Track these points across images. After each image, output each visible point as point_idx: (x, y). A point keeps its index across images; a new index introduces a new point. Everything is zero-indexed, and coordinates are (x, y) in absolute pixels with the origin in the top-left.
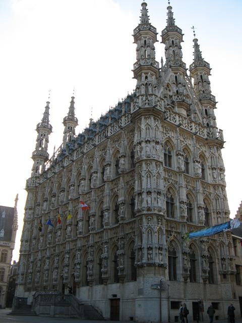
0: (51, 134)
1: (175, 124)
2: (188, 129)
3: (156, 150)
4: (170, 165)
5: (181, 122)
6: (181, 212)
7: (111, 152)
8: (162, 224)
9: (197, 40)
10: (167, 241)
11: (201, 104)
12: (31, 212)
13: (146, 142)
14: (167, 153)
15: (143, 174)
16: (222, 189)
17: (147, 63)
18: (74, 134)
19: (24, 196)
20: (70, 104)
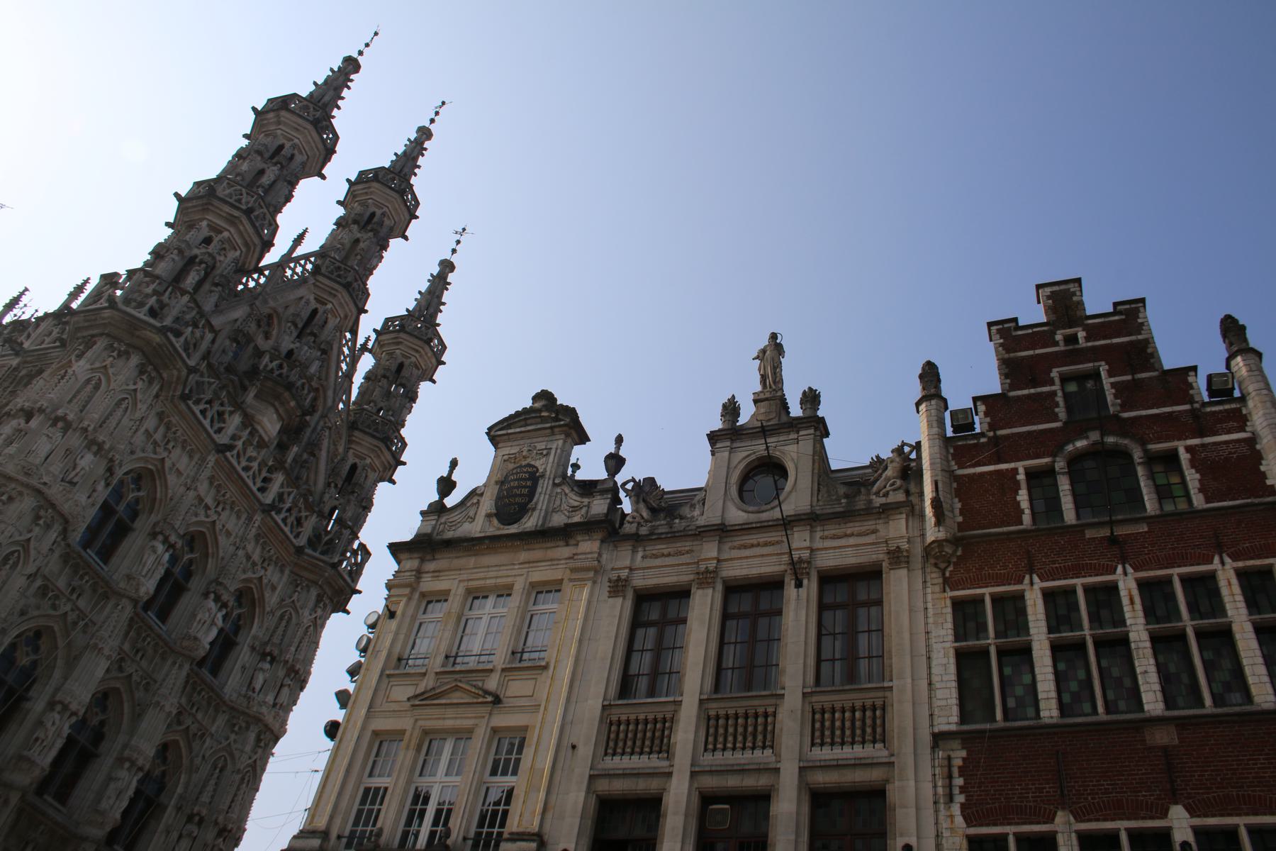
1: (215, 436)
2: (250, 483)
3: (74, 468)
4: (106, 554)
11: (350, 442)
13: (56, 421)
14: (121, 508)
16: (258, 740)
17: (239, 201)
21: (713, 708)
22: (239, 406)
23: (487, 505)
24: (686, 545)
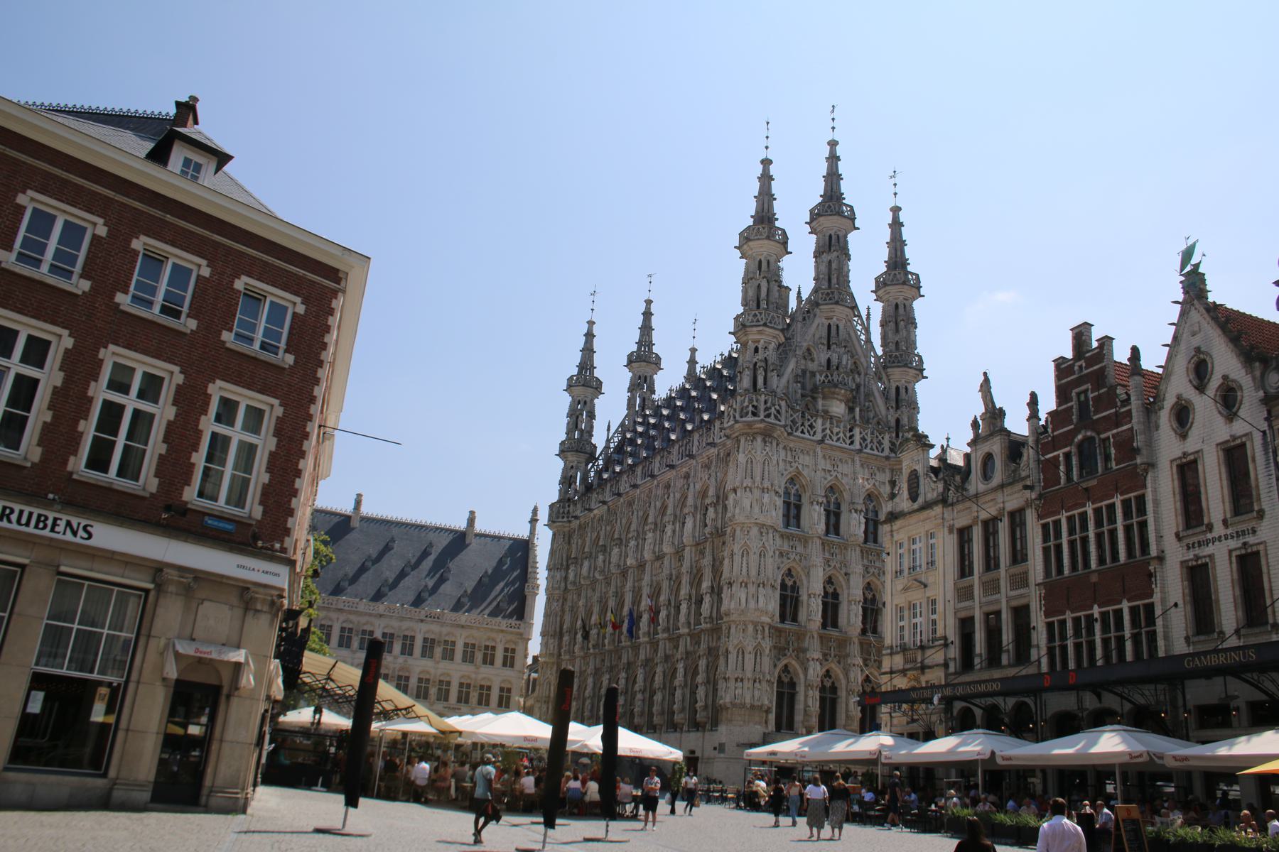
6: (812, 611)
7: (698, 486)
12: (558, 575)
18: (653, 392)
21: (984, 579)
23: (905, 494)
24: (968, 504)
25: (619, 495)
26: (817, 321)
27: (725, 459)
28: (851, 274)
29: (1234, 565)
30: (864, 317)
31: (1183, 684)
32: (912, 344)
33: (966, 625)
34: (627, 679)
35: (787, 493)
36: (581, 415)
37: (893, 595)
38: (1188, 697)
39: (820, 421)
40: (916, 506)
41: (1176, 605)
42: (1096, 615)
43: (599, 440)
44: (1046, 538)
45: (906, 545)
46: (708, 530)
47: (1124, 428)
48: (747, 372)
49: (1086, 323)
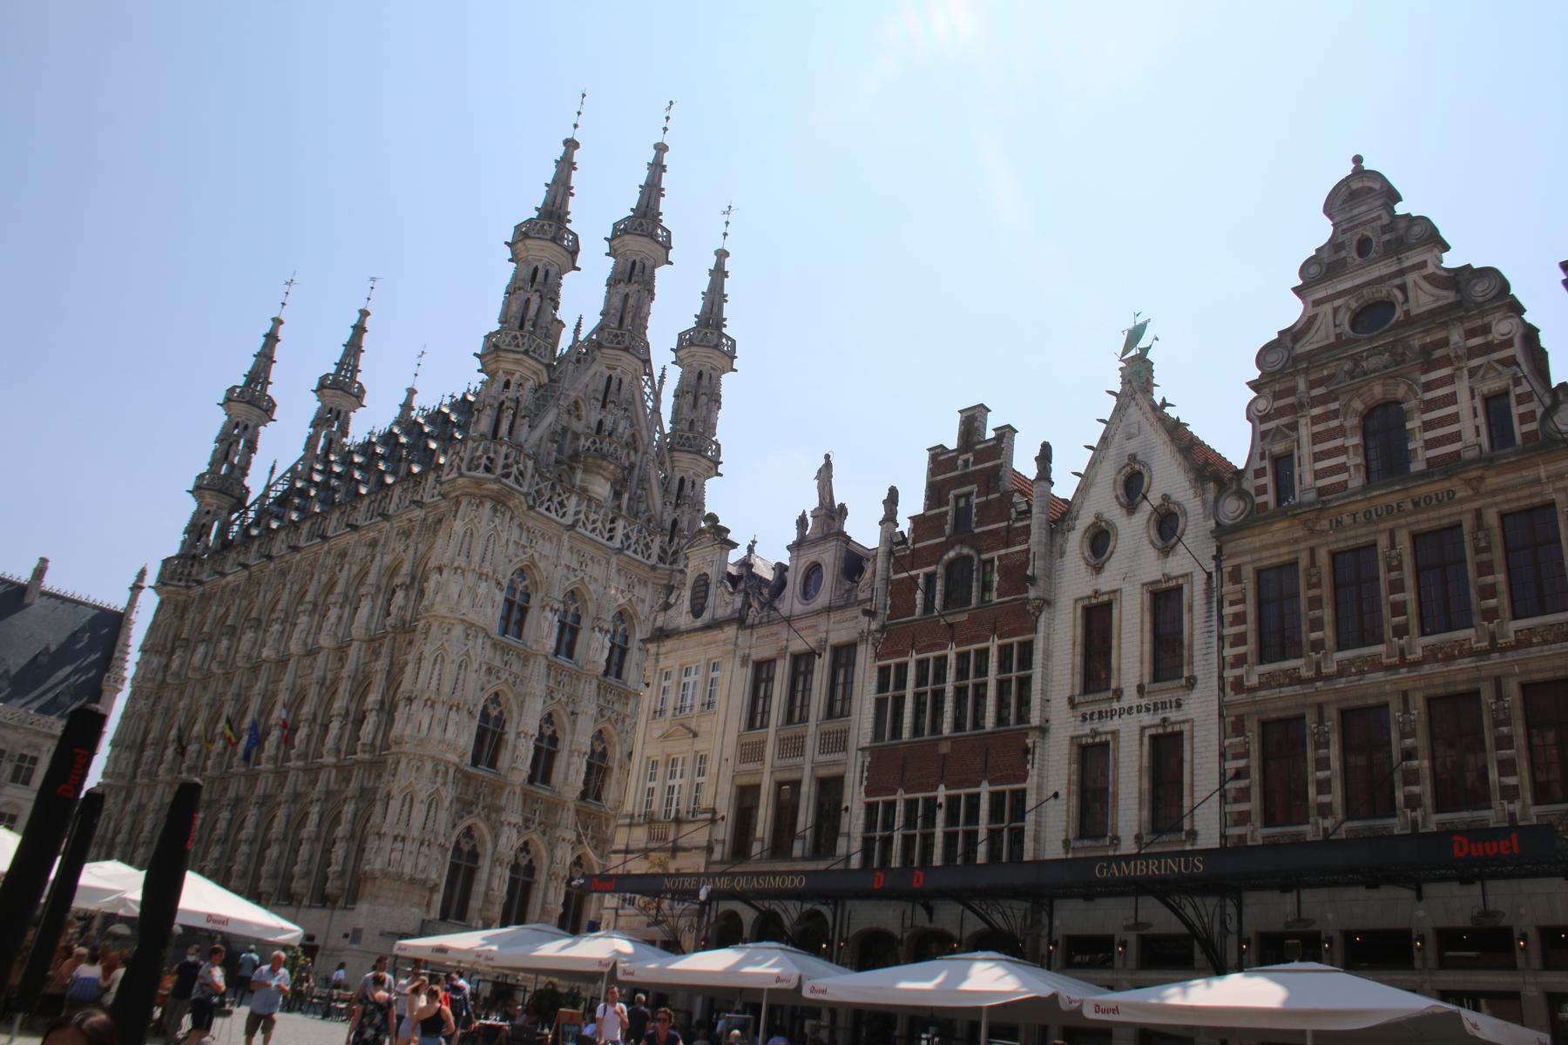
0: (270, 424)
2: (599, 539)
5: (582, 516)
6: (519, 756)
7: (388, 559)
8: (445, 784)
9: (727, 254)
10: (454, 826)
12: (155, 661)
15: (428, 650)
18: (345, 434)
19: (149, 602)
20: (351, 331)
21: (783, 734)
22: (571, 490)
24: (774, 629)
25: (270, 558)
26: (595, 368)
27: (434, 527)
28: (650, 318)
29: (1146, 748)
30: (657, 379)
31: (1051, 906)
32: (711, 427)
33: (746, 797)
34: (230, 821)
35: (512, 588)
36: (237, 441)
37: (646, 740)
38: (1057, 923)
39: (574, 499)
40: (699, 623)
41: (1056, 795)
42: (941, 799)
43: (255, 482)
44: (882, 686)
45: (675, 677)
46: (390, 621)
47: (1018, 548)
48: (488, 411)
49: (982, 406)
